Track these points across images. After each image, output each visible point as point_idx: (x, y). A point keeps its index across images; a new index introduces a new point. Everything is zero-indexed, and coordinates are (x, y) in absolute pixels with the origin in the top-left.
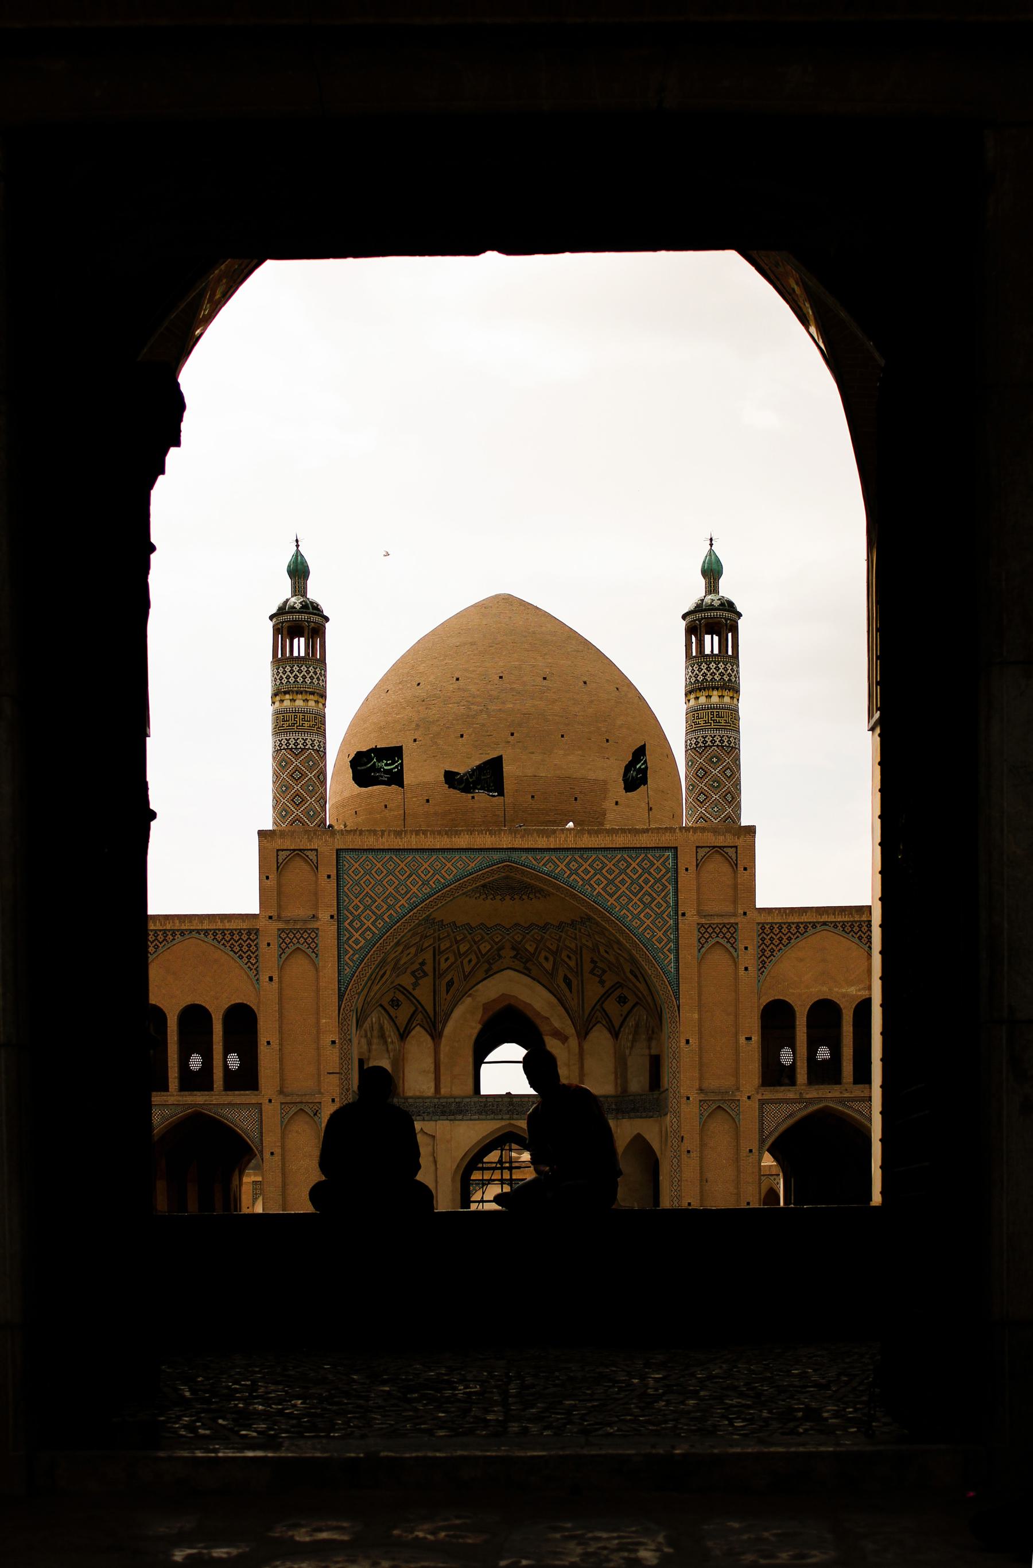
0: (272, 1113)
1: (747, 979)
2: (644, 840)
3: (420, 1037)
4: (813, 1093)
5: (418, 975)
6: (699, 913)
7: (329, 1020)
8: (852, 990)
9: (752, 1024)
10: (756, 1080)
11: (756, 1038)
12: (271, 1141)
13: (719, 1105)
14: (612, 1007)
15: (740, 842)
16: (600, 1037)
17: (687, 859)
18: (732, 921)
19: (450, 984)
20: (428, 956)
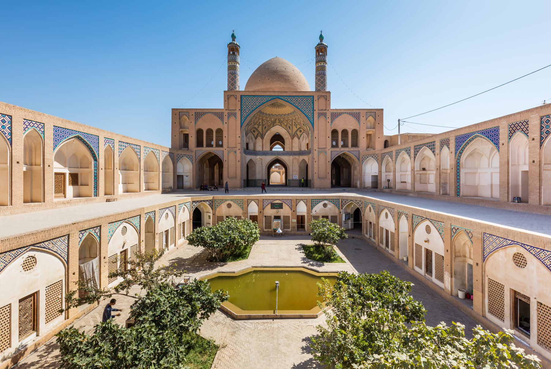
0: (226, 153)
1: (329, 125)
2: (307, 94)
3: (259, 138)
4: (343, 149)
5: (259, 125)
6: (319, 110)
7: (238, 132)
8: (351, 127)
9: (329, 134)
10: (330, 146)
11: (330, 137)
12: (225, 158)
13: (322, 150)
14: (298, 133)
15: (327, 95)
16: (296, 139)
17: (316, 98)
18: (325, 111)
19: (265, 127)
20: (261, 121)
